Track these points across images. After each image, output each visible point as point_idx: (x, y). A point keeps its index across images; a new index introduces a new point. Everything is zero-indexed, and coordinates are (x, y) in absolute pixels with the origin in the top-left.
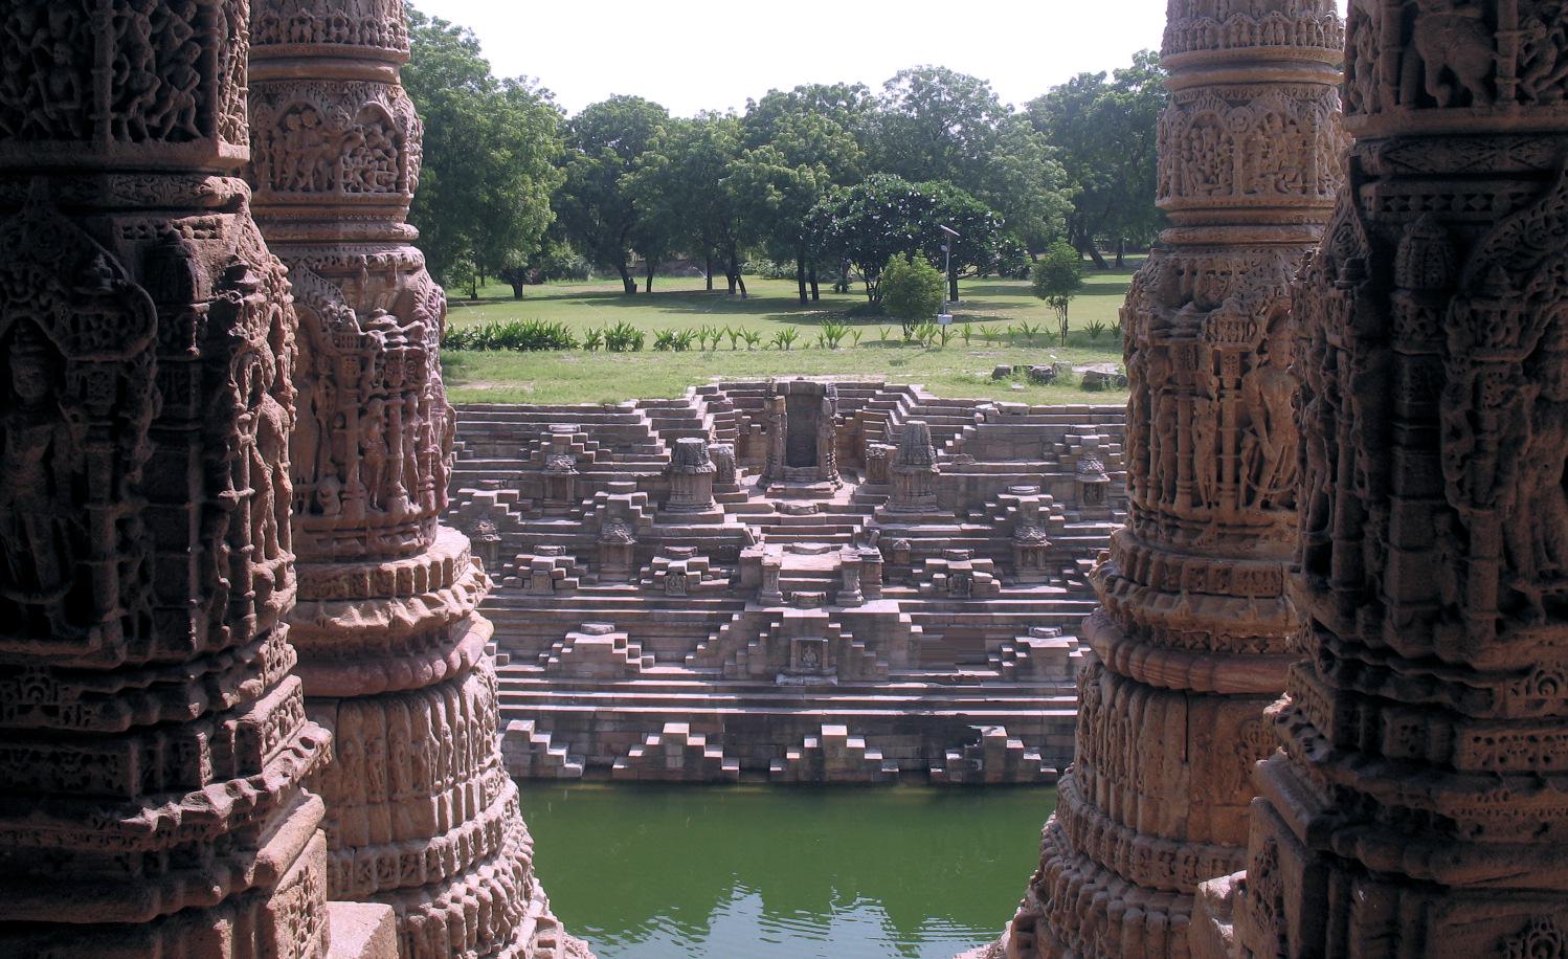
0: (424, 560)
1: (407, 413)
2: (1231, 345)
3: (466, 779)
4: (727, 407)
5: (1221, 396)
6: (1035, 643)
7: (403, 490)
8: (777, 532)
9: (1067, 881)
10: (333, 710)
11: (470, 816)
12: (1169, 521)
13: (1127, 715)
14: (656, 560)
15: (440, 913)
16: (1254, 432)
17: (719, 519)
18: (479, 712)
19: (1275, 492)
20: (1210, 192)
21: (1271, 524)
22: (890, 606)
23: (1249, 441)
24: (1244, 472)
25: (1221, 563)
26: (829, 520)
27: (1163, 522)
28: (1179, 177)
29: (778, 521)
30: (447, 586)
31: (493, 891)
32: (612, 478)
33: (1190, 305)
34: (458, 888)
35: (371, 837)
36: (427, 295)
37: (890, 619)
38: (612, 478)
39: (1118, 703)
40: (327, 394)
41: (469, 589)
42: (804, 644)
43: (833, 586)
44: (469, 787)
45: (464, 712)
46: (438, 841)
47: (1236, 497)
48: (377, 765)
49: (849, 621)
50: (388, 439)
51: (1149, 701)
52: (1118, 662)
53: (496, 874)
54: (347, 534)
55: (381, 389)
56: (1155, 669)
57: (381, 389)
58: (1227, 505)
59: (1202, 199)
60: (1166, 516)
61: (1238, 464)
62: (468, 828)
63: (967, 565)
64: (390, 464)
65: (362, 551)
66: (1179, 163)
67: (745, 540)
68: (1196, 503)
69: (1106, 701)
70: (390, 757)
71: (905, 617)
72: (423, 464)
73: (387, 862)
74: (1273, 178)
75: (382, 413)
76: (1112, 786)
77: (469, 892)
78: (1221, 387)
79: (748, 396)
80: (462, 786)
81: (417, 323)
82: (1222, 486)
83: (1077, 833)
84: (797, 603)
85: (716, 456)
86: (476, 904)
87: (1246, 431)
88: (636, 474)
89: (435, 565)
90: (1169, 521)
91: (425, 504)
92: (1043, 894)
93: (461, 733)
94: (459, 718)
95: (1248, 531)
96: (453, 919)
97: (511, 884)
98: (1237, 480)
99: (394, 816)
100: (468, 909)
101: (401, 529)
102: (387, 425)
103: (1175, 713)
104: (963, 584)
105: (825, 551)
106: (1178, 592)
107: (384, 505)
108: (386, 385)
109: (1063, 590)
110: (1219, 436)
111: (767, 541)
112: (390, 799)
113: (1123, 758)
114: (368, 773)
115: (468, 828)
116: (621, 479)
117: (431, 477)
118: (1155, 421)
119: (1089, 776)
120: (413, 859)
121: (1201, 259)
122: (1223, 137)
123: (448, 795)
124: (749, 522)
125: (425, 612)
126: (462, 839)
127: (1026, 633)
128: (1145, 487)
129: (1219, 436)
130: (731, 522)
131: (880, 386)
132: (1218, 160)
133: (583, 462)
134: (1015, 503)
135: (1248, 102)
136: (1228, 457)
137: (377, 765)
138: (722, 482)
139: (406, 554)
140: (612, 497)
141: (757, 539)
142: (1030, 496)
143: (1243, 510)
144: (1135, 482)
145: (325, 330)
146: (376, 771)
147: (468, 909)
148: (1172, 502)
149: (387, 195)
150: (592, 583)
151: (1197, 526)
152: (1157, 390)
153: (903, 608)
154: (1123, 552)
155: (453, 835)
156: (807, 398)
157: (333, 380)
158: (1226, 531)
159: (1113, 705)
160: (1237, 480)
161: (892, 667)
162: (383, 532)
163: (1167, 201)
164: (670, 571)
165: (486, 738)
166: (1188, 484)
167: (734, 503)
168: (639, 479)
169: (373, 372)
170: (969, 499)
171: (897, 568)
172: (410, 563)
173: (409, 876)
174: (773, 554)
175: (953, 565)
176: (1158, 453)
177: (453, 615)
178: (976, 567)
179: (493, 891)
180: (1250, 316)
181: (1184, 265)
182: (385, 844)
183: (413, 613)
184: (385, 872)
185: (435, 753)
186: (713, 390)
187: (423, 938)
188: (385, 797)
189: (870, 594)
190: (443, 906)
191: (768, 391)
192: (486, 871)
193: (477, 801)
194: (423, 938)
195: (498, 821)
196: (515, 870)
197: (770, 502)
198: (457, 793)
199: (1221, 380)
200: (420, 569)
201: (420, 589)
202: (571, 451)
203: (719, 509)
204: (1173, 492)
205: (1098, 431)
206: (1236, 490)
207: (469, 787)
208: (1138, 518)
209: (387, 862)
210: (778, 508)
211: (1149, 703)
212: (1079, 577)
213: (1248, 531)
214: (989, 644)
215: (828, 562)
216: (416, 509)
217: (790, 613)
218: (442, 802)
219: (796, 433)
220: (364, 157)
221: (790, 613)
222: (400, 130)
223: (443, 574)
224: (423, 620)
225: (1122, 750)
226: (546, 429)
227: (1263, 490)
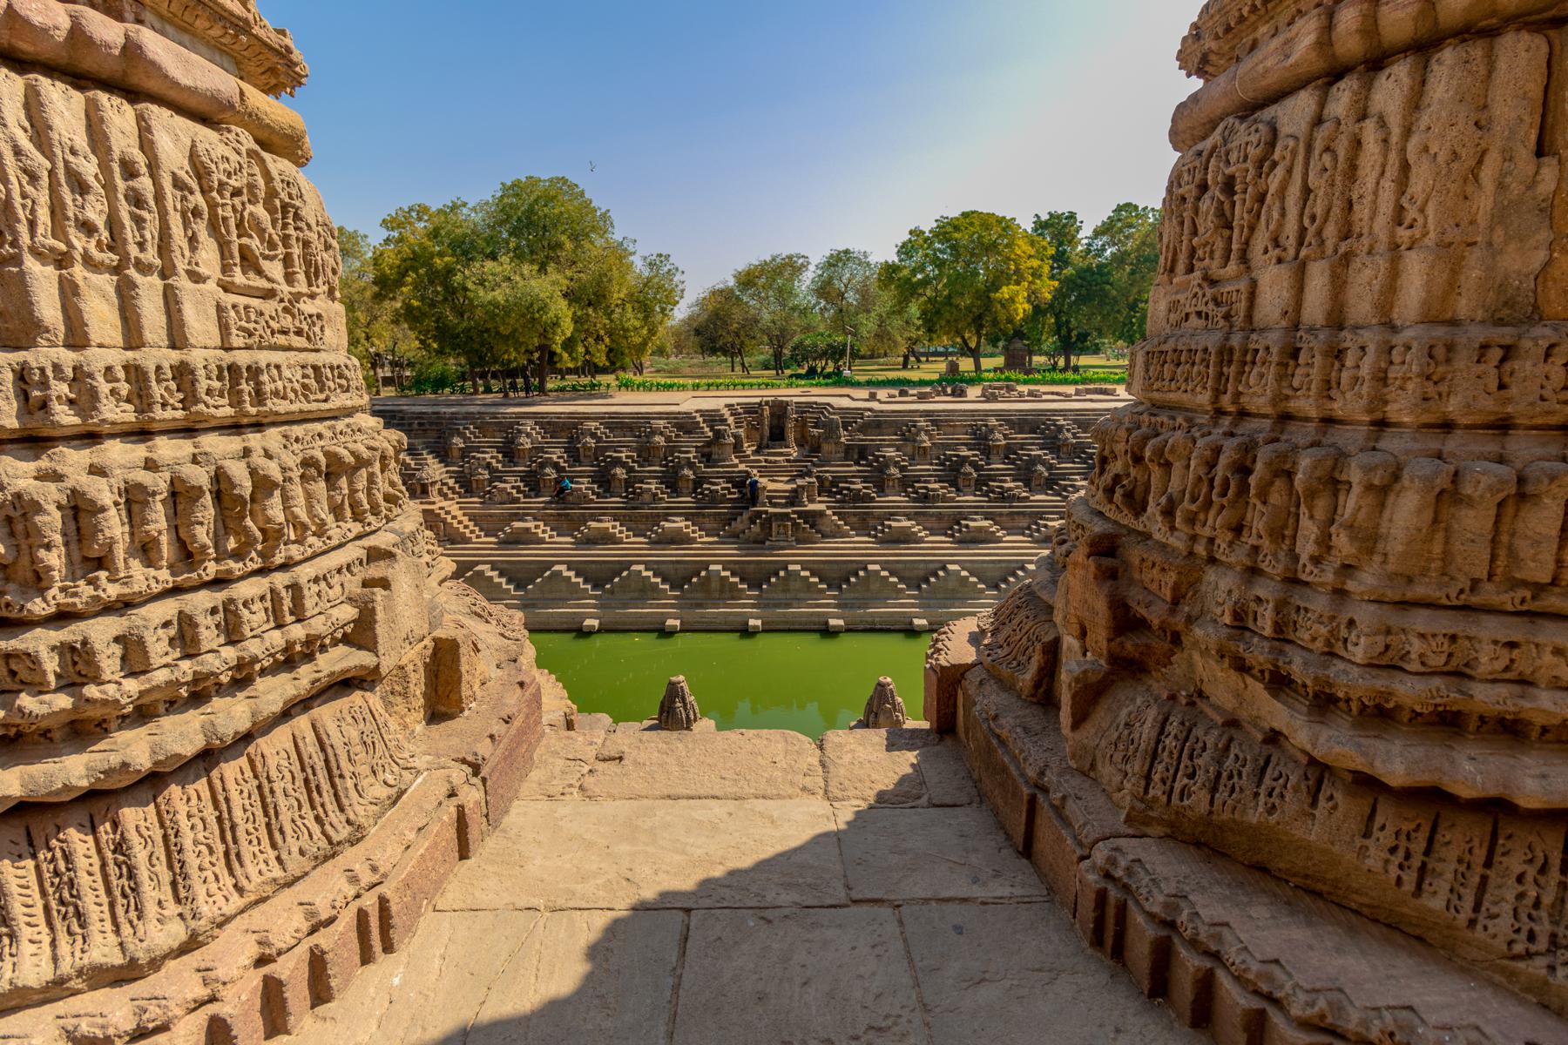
6: (894, 524)
8: (764, 471)
22: (822, 507)
37: (821, 514)
43: (793, 498)
49: (800, 514)
63: (859, 486)
71: (829, 512)
79: (751, 410)
84: (775, 505)
85: (736, 436)
104: (857, 497)
130: (742, 467)
133: (668, 439)
138: (737, 447)
142: (891, 452)
156: (780, 409)
167: (743, 458)
170: (859, 453)
171: (826, 487)
189: (812, 501)
202: (661, 434)
214: (872, 523)
217: (771, 510)
221: (771, 510)
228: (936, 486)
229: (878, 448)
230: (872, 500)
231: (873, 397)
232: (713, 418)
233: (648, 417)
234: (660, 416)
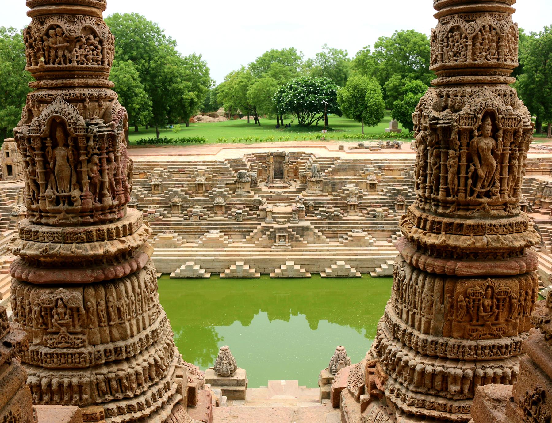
0: (120, 224)
1: (109, 161)
2: (465, 127)
3: (142, 314)
4: (254, 160)
5: (460, 149)
7: (109, 195)
8: (270, 200)
9: (391, 350)
10: (81, 289)
11: (144, 329)
12: (435, 203)
13: (417, 284)
14: (232, 210)
15: (131, 371)
16: (474, 165)
17: (252, 196)
18: (146, 286)
19: (483, 190)
20: (456, 60)
21: (481, 204)
22: (308, 224)
23: (472, 168)
24: (470, 181)
25: (458, 221)
26: (287, 196)
27: (433, 203)
28: (442, 55)
29: (271, 197)
30: (131, 234)
31: (155, 360)
32: (217, 184)
33: (447, 110)
34: (140, 359)
35: (101, 341)
36: (117, 111)
38: (217, 184)
39: (413, 279)
40: (73, 154)
41: (141, 235)
42: (280, 236)
44: (143, 318)
45: (140, 287)
46: (130, 341)
47: (466, 193)
48: (102, 311)
50: (101, 172)
51: (427, 278)
52: (414, 262)
53: (156, 351)
54: (85, 214)
55: (96, 151)
56: (423, 260)
57: (96, 151)
58: (461, 194)
59: (453, 63)
60: (434, 200)
61: (467, 179)
62: (144, 334)
63: (332, 210)
64: (102, 183)
65: (92, 221)
66: (442, 48)
67: (260, 203)
68: (448, 195)
69: (408, 278)
70: (107, 307)
71: (313, 227)
72: (117, 182)
73: (108, 351)
74: (484, 54)
75: (97, 161)
76: (411, 313)
77: (144, 360)
78: (461, 146)
79: (261, 157)
80: (140, 317)
81: (112, 122)
82: (460, 188)
83: (394, 330)
84: (278, 223)
85: (251, 176)
86: (147, 366)
87: (471, 164)
88: (226, 182)
89: (124, 226)
90: (435, 203)
91: (120, 200)
92: (380, 354)
93: (138, 295)
94: (137, 290)
95: (471, 207)
96: (137, 374)
97: (162, 356)
98: (466, 185)
99: (111, 332)
100: (144, 369)
101: (109, 211)
102: (100, 166)
103: (438, 284)
104: (331, 217)
105: (288, 206)
106: (440, 233)
107: (101, 201)
108: (99, 149)
109: (364, 218)
110: (459, 167)
111: (268, 203)
112: (108, 324)
113: (415, 302)
114: (98, 314)
115: (144, 334)
116: (220, 184)
117: (122, 189)
118: (431, 160)
119: (400, 307)
120: (119, 349)
121: (452, 90)
122: (463, 36)
123: (134, 322)
124: (262, 197)
125: (121, 246)
126: (141, 340)
127: (351, 231)
128: (424, 188)
129: (459, 167)
130: (256, 197)
131: (304, 153)
132: (460, 46)
134: (348, 190)
135: (475, 20)
136: (463, 175)
137: (102, 311)
138: (253, 183)
139: (111, 221)
140: (218, 190)
141: (265, 203)
142: (351, 187)
143: (469, 198)
144: (420, 186)
145: (70, 125)
146: (101, 314)
147: (144, 369)
148: (438, 195)
149: (97, 66)
150: (212, 217)
151: (448, 205)
152: (431, 147)
153: (312, 224)
154: (415, 215)
155: (136, 339)
157: (76, 148)
158: (461, 207)
159: (411, 279)
160: (466, 185)
161: (308, 243)
162: (100, 213)
163: (435, 66)
164: (237, 213)
165: (152, 295)
166: (444, 187)
168: (227, 184)
169: (91, 143)
172: (113, 226)
173: (118, 356)
174: (269, 207)
175: (328, 210)
176: (431, 174)
177: (132, 247)
178: (335, 211)
179: (155, 360)
180: (474, 115)
181: (444, 93)
182: (108, 343)
183: (113, 247)
184: (108, 355)
185: (127, 305)
186: (250, 155)
187: (125, 381)
188: (106, 324)
189: (300, 219)
190: (133, 368)
191: (268, 155)
192: (152, 351)
193: (147, 323)
194: (125, 381)
195: (157, 330)
196: (165, 348)
197: (269, 190)
198: (138, 320)
199: (461, 143)
200: (124, 226)
201: (118, 235)
203: (252, 193)
204: (437, 190)
205: (374, 167)
206: (466, 190)
207: (143, 318)
208: (421, 201)
209: (108, 351)
210: (271, 192)
211: (428, 280)
212: (368, 214)
213: (471, 207)
215: (289, 209)
216: (116, 203)
218: (131, 325)
219: (278, 167)
220: (85, 49)
222: (102, 38)
223: (129, 230)
224: (119, 250)
225: (415, 298)
226: (196, 168)
227: (478, 189)
228: (381, 209)
229: (343, 184)
230: (340, 219)
231: (341, 148)
232: (236, 164)
233: (195, 164)
234: (204, 163)
